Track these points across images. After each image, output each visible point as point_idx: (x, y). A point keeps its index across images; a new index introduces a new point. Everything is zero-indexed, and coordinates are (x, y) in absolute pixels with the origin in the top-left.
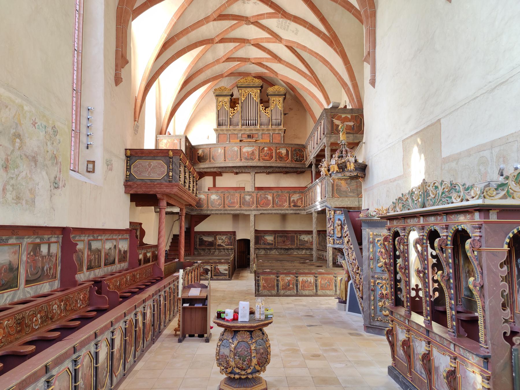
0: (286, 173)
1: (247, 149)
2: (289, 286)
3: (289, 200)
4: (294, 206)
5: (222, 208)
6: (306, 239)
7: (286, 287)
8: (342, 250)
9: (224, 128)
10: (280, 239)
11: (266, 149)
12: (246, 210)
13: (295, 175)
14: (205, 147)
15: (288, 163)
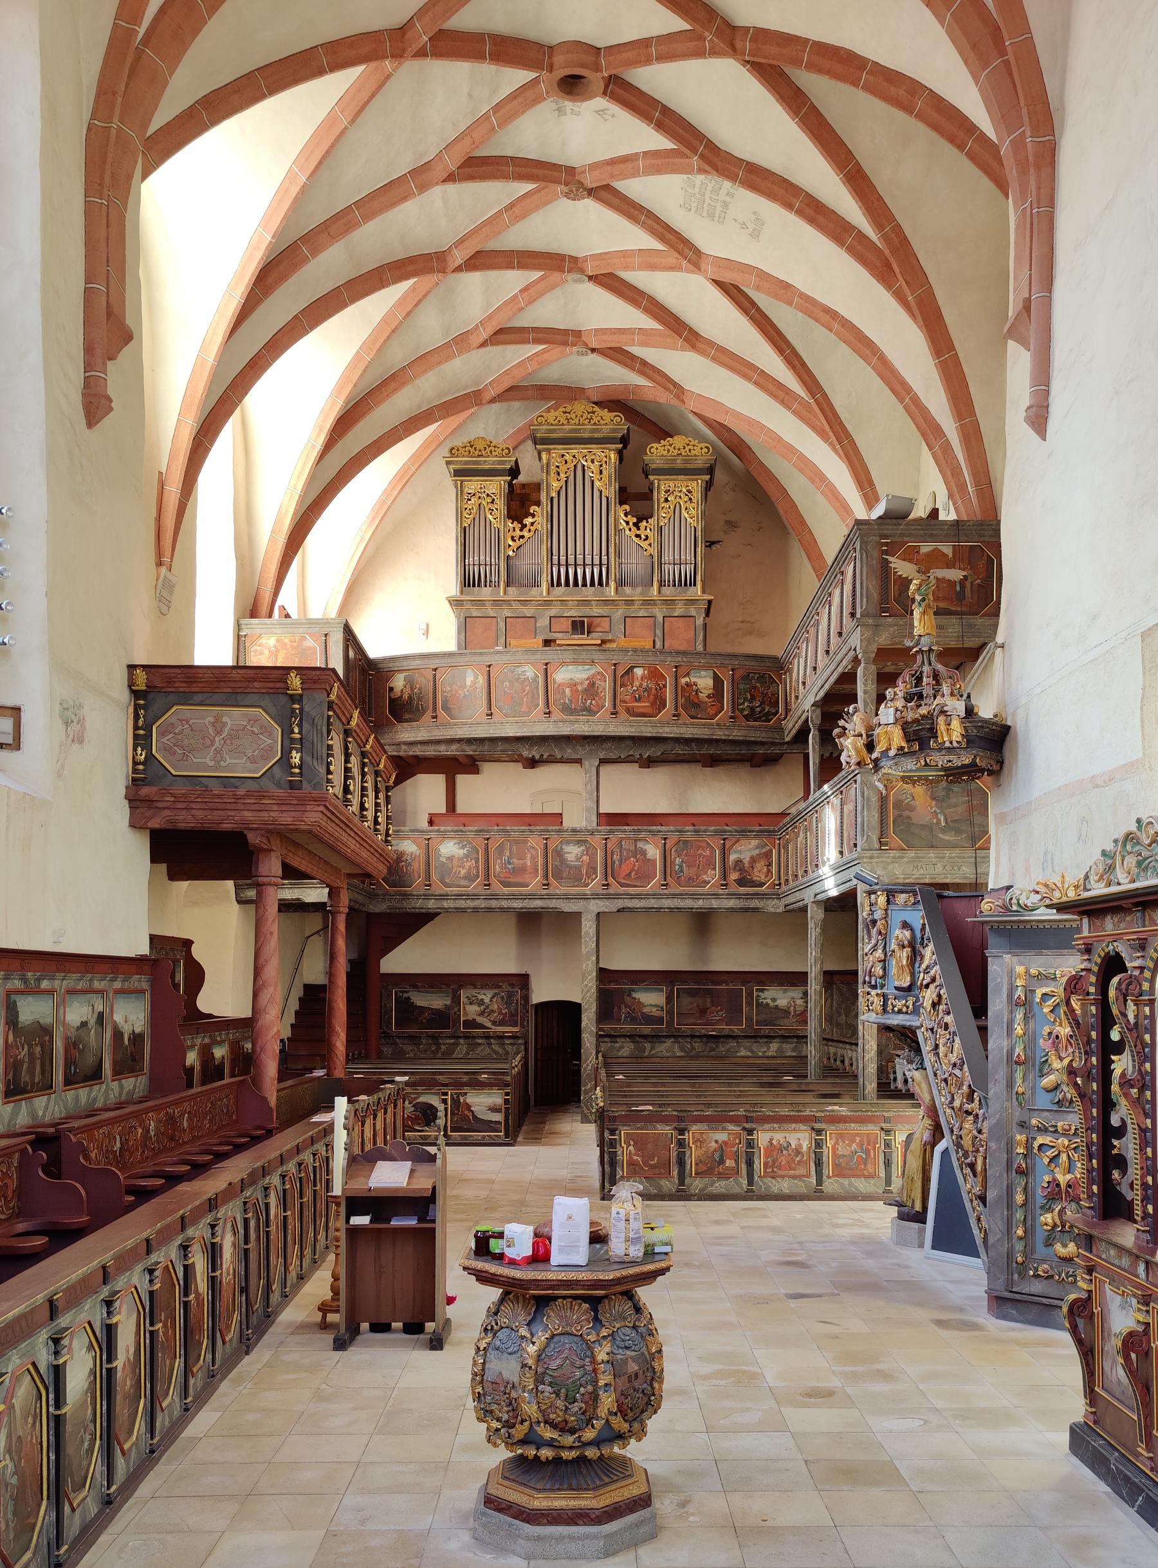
2: (722, 1161)
4: (741, 882)
5: (481, 890)
6: (782, 1002)
7: (712, 1166)
8: (914, 1033)
9: (485, 593)
11: (639, 672)
12: (567, 897)
13: (744, 770)
15: (720, 726)
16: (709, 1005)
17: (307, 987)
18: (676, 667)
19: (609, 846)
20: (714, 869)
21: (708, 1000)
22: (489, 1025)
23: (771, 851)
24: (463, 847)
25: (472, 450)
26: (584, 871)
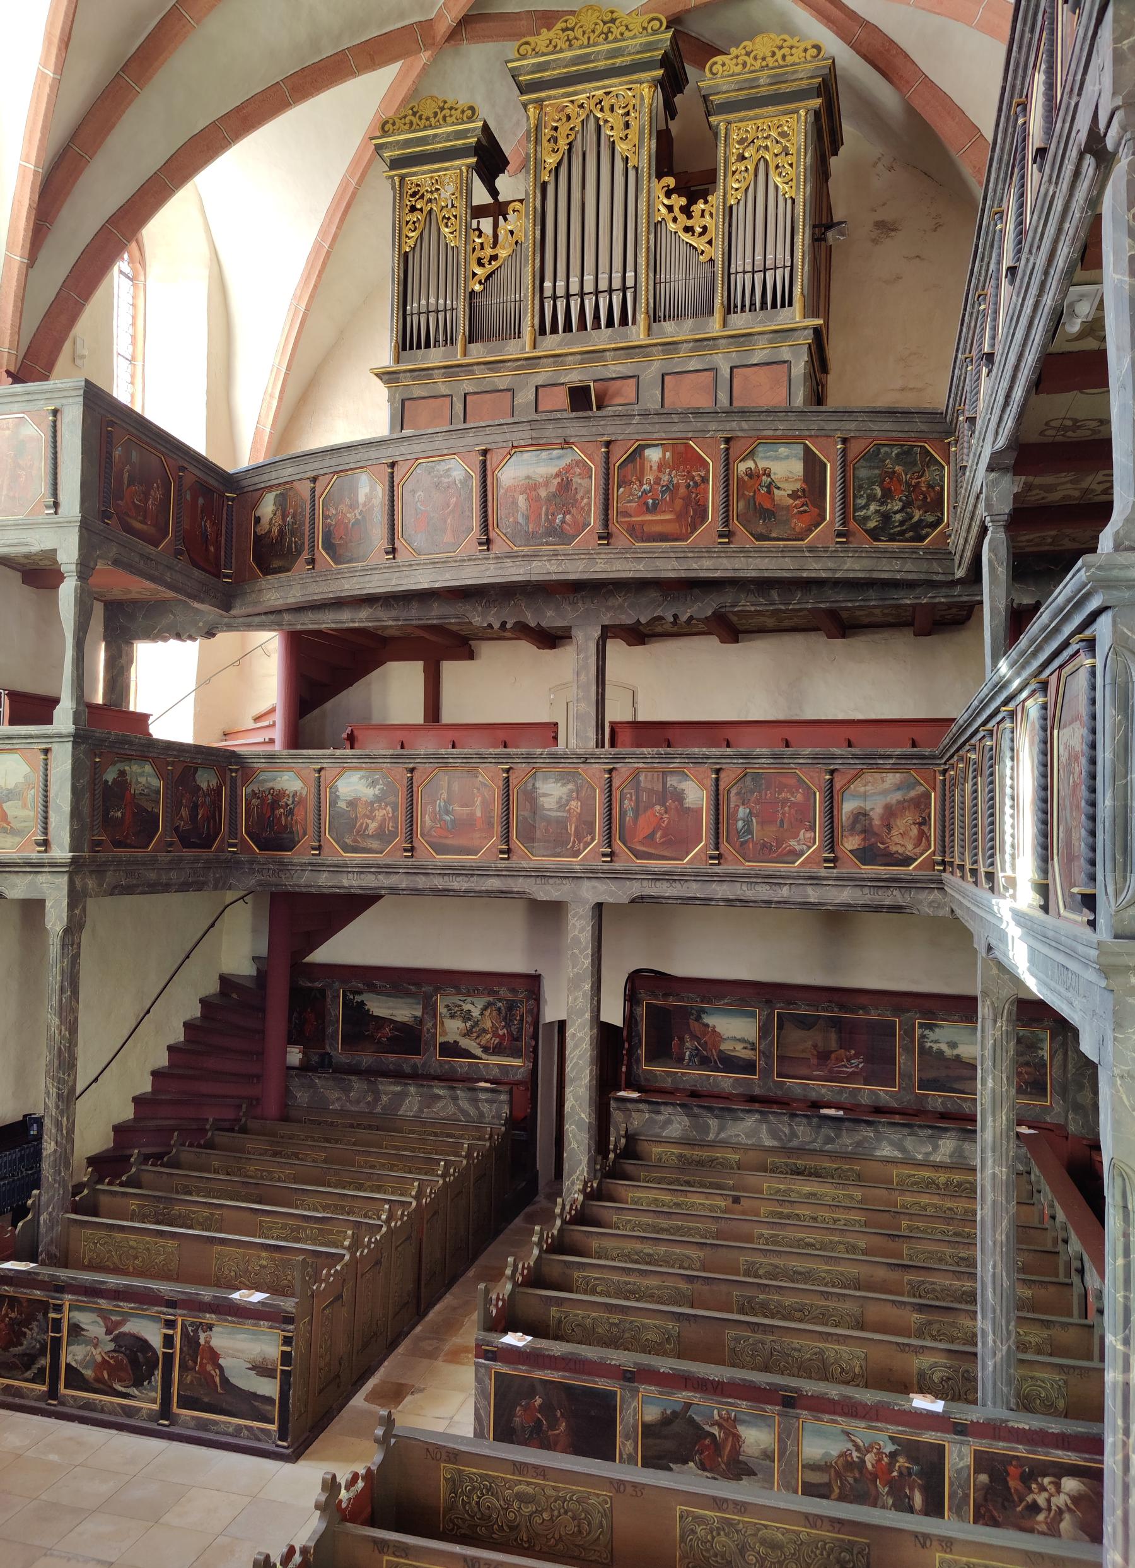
0: (841, 626)
1: (523, 471)
4: (866, 855)
5: (400, 858)
10: (803, 1042)
11: (654, 455)
12: (541, 875)
13: (902, 642)
14: (287, 473)
16: (834, 1045)
17: (224, 980)
18: (728, 441)
19: (616, 783)
20: (813, 828)
22: (478, 1051)
24: (373, 784)
25: (415, 120)
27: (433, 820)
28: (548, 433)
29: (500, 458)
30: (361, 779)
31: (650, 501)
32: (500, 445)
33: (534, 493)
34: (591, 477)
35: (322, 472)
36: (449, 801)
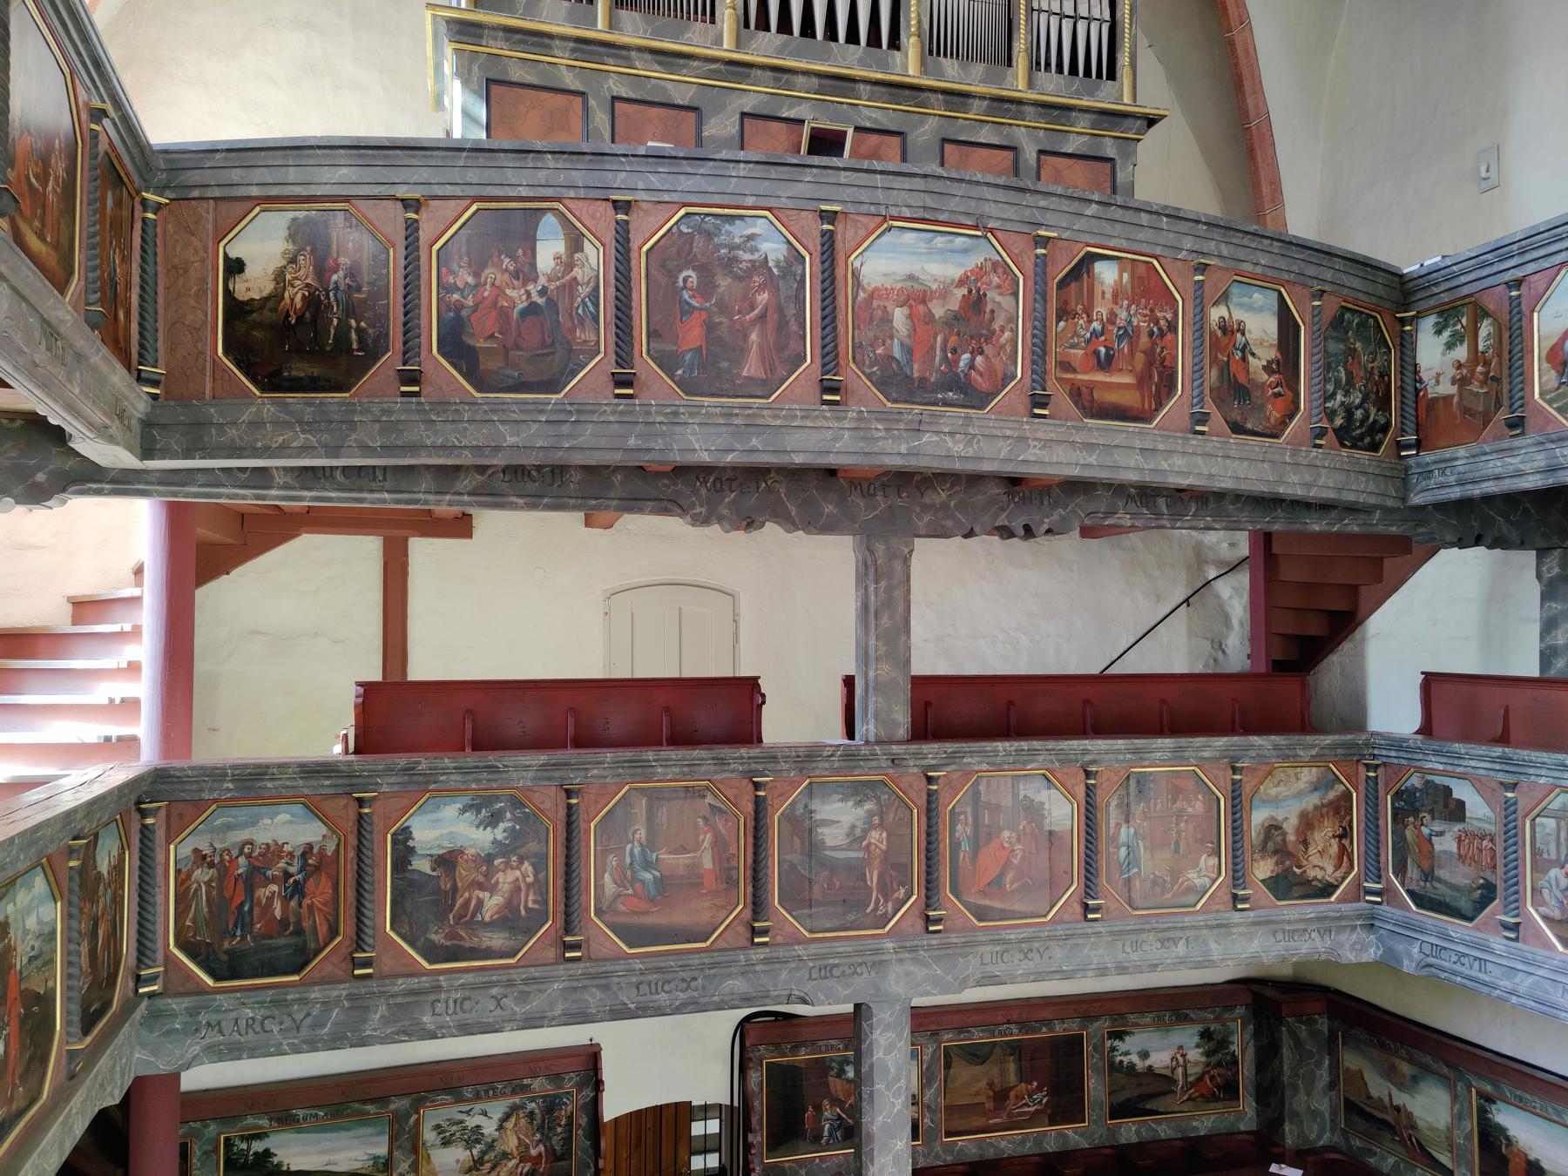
3: (1237, 830)
6: (1160, 1059)
11: (1107, 274)
21: (1012, 1067)
23: (1347, 796)
26: (873, 878)
27: (620, 882)
28: (953, 204)
29: (862, 233)
30: (463, 811)
31: (1103, 350)
32: (864, 208)
33: (921, 308)
34: (1016, 294)
35: (438, 191)
36: (651, 844)
